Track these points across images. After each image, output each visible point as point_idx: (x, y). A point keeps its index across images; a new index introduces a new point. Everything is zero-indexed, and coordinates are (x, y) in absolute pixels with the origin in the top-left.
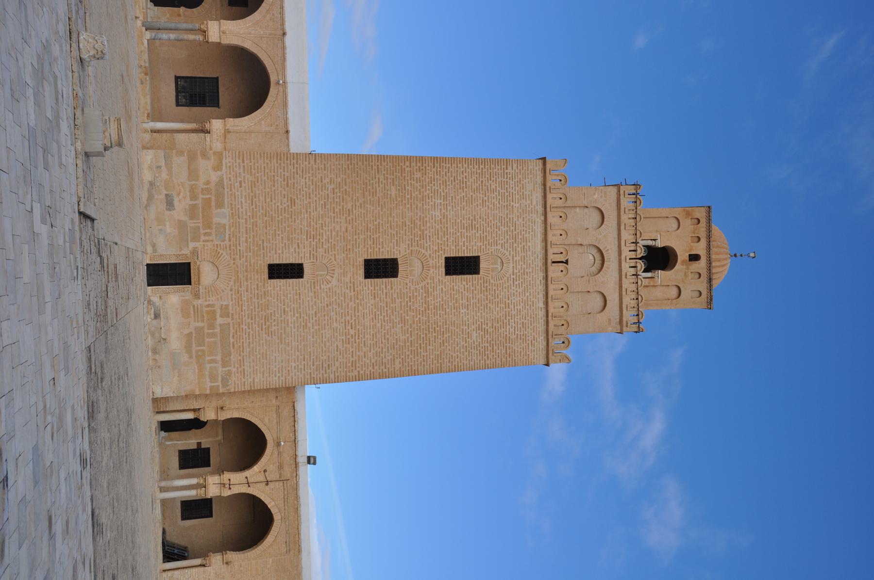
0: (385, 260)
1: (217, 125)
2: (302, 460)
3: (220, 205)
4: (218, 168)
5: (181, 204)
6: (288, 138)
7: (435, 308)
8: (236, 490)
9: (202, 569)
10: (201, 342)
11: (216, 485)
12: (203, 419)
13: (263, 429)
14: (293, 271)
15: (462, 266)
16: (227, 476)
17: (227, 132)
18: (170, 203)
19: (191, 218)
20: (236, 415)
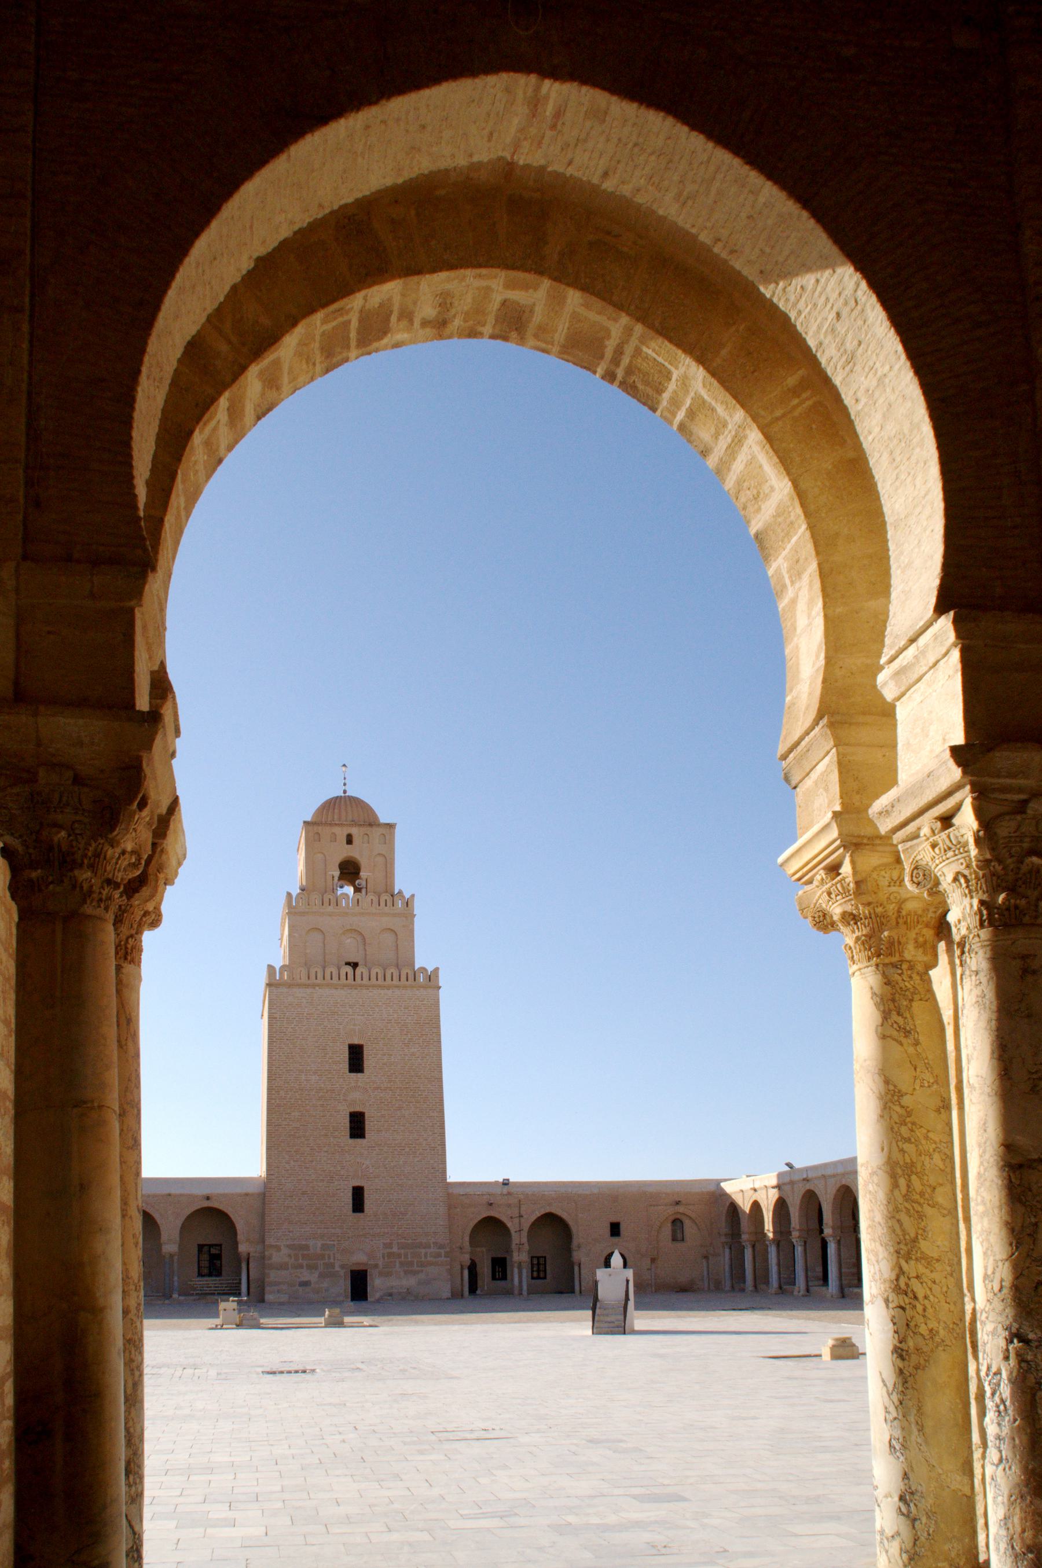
0: (351, 1122)
1: (243, 1248)
2: (505, 1190)
3: (307, 1247)
4: (278, 1248)
5: (306, 1275)
6: (253, 1195)
7: (390, 1082)
8: (525, 1240)
9: (582, 1266)
10: (411, 1263)
11: (520, 1257)
12: (468, 1263)
13: (480, 1218)
14: (358, 1194)
15: (356, 1058)
16: (514, 1246)
17: (248, 1240)
18: (305, 1284)
19: (316, 1269)
20: (467, 1239)
